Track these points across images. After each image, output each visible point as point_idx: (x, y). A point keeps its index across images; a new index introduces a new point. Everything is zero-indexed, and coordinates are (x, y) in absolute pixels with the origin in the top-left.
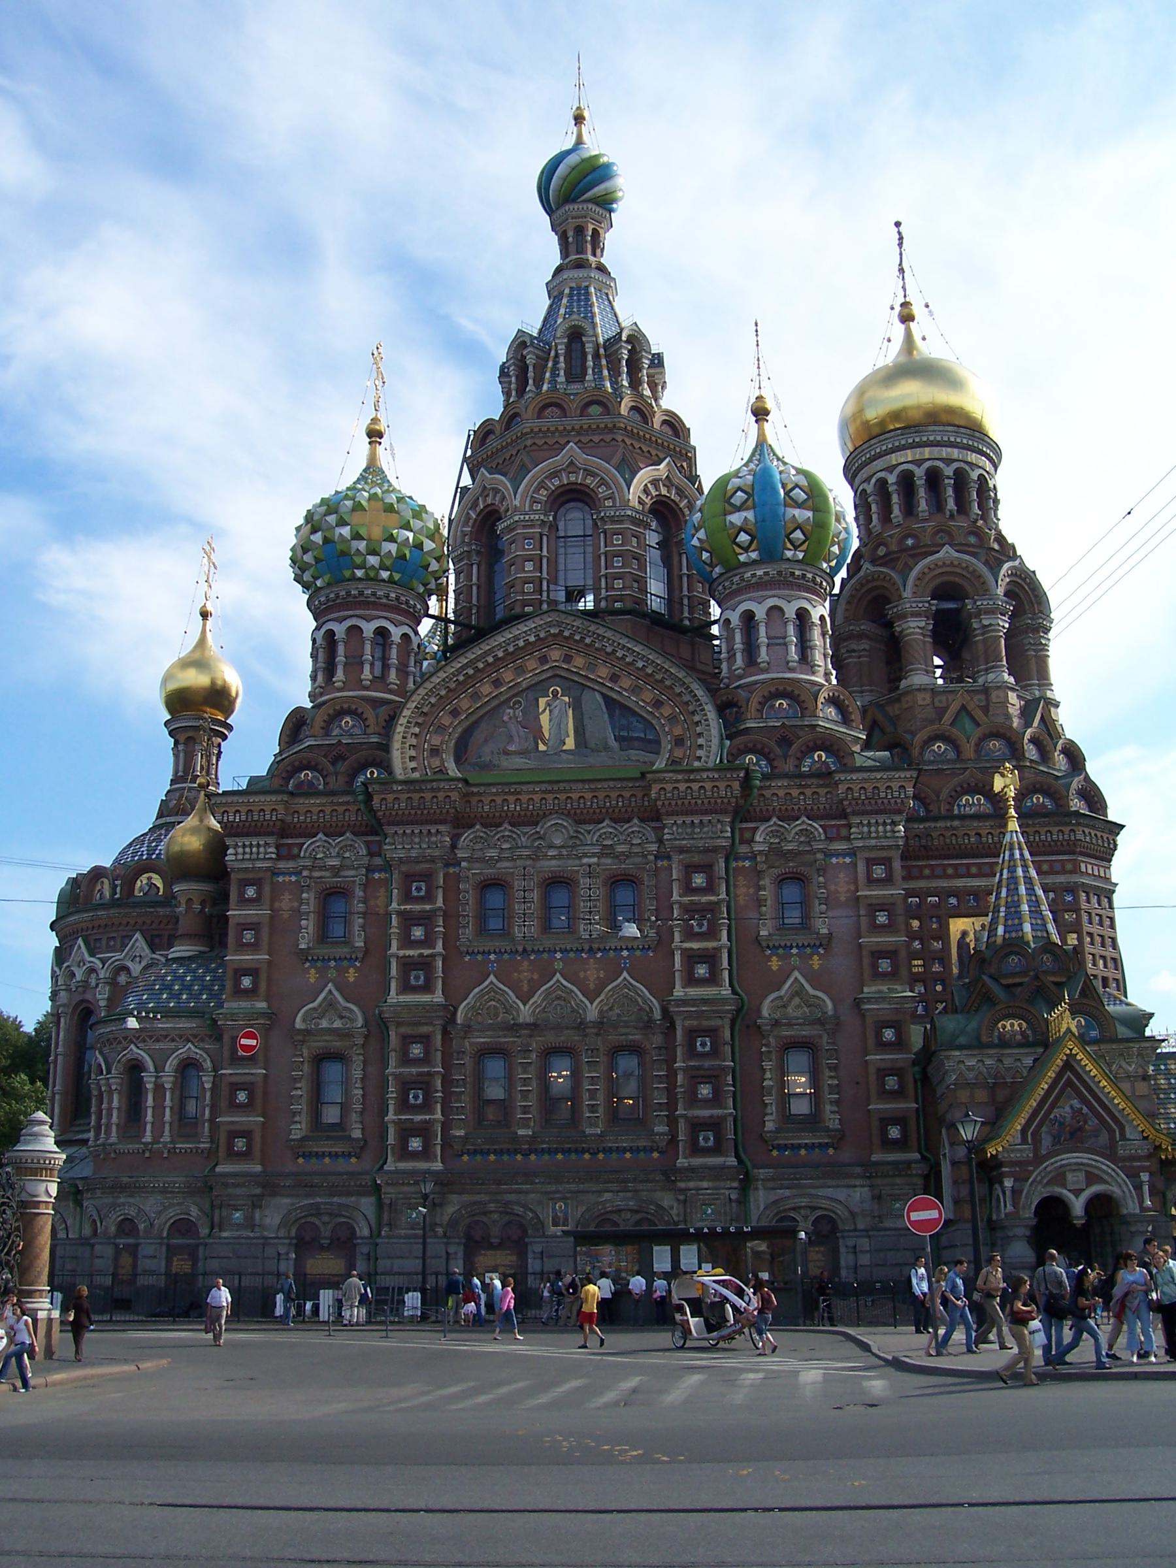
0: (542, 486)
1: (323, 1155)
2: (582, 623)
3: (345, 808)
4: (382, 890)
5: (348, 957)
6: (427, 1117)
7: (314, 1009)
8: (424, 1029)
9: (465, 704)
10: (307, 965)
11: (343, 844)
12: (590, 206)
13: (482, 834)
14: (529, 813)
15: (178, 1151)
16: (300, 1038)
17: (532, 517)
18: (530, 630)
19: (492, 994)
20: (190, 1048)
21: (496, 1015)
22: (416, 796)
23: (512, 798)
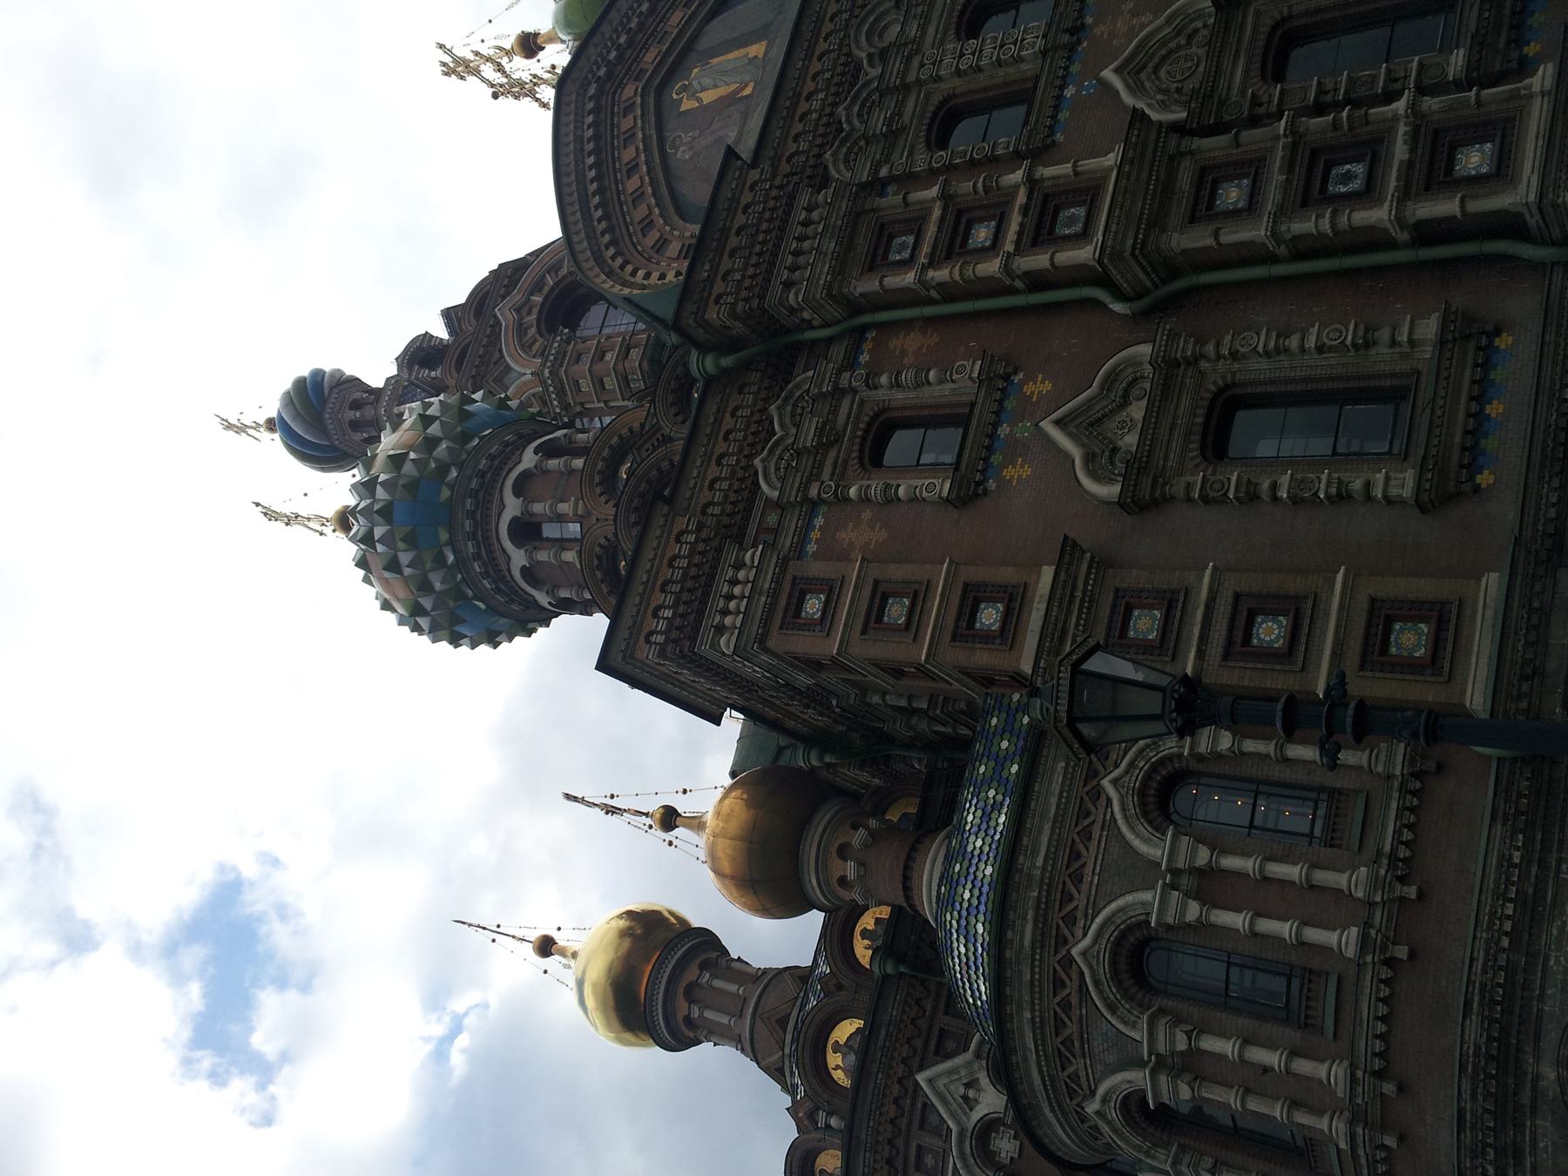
0: (526, 347)
1: (1479, 417)
2: (596, 45)
3: (728, 414)
4: (895, 343)
5: (998, 395)
6: (1402, 129)
7: (1090, 458)
8: (1185, 178)
9: (640, 213)
10: (992, 485)
11: (788, 420)
12: (336, 390)
13: (844, 150)
14: (836, 79)
15: (1403, 852)
16: (1146, 482)
17: (553, 352)
18: (576, 121)
19: (1143, 76)
20: (1115, 782)
21: (1187, 58)
22: (733, 241)
23: (803, 107)
